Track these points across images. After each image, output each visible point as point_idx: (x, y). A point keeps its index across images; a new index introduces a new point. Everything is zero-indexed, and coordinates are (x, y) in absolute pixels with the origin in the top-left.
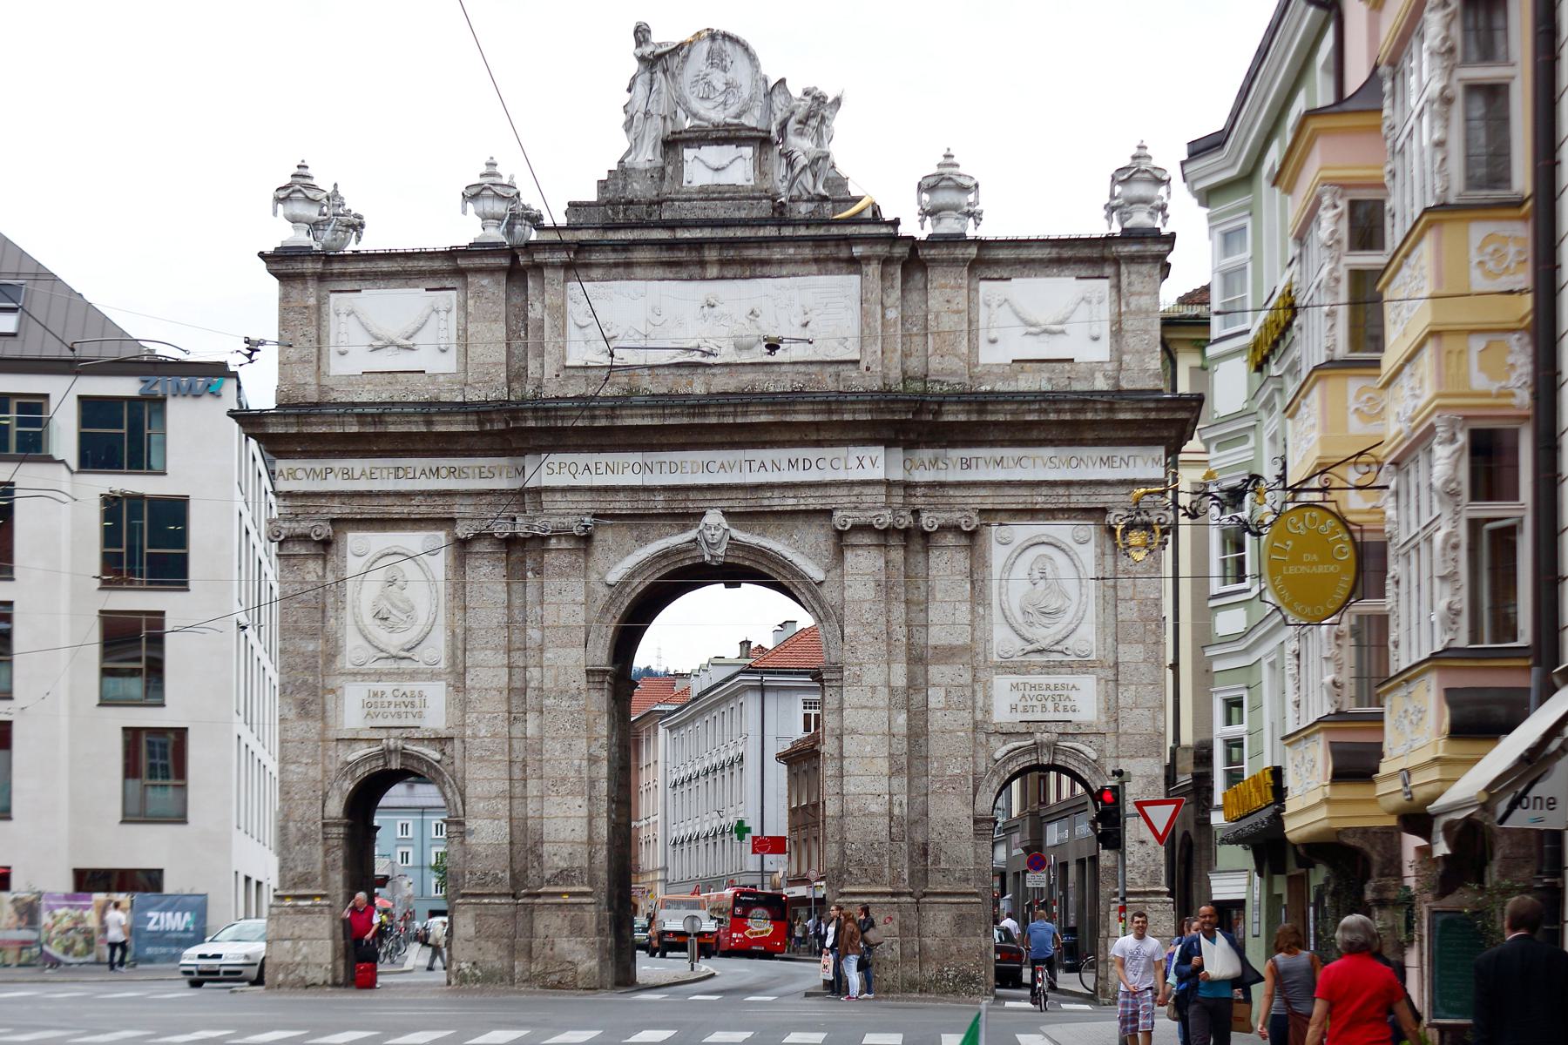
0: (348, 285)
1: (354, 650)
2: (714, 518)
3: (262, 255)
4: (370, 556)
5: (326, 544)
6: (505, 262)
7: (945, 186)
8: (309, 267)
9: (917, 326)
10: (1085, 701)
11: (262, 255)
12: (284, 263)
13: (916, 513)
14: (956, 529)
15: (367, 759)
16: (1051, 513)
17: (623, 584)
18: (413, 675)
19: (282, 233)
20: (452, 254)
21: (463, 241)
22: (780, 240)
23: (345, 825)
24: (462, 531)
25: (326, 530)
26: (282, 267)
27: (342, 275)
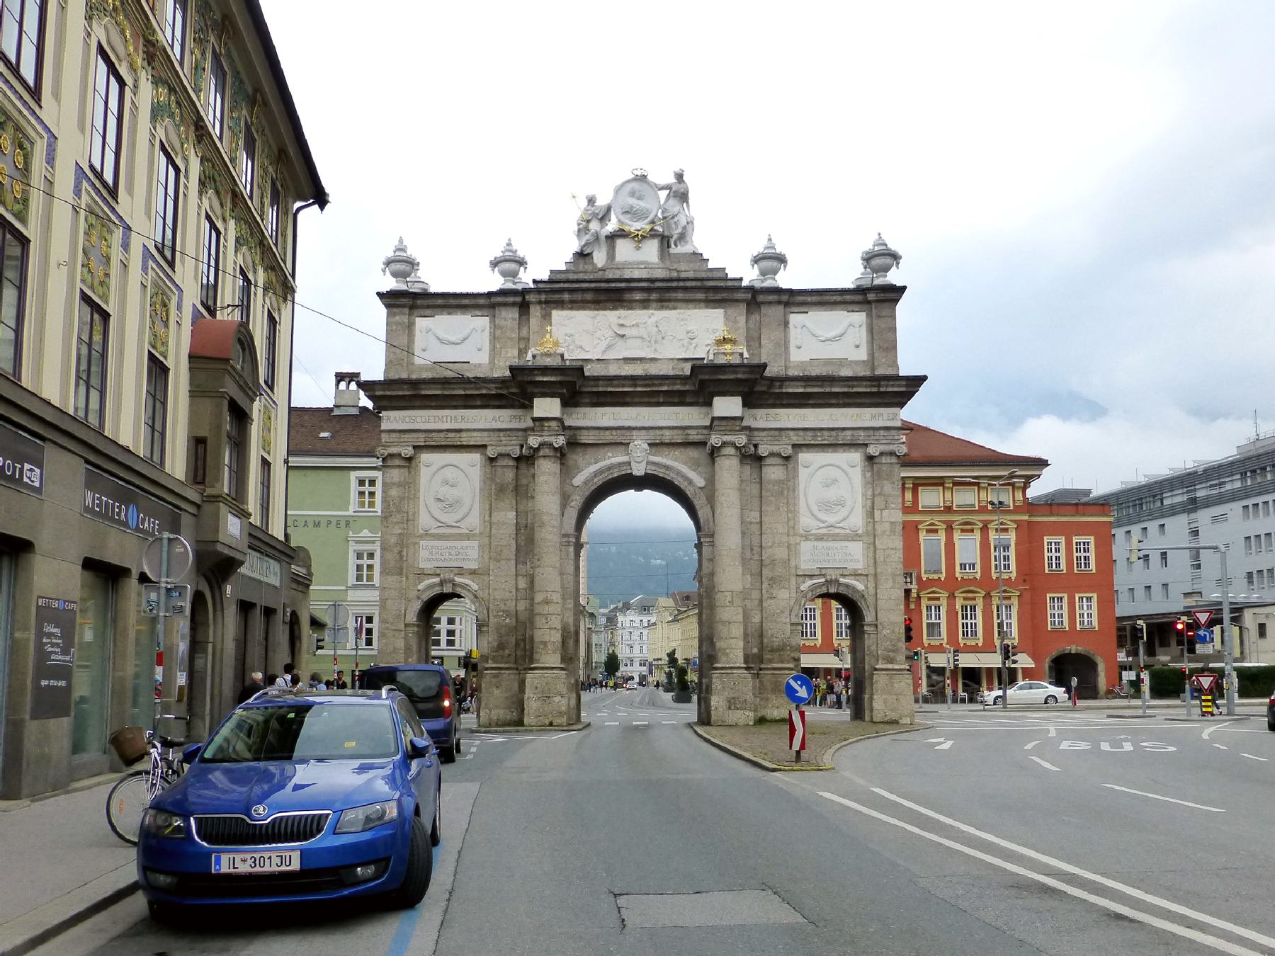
0: (428, 312)
1: (424, 521)
2: (639, 445)
3: (378, 294)
4: (434, 468)
5: (410, 459)
6: (519, 299)
7: (772, 260)
8: (403, 301)
9: (754, 340)
10: (854, 556)
11: (378, 294)
12: (390, 299)
13: (756, 446)
14: (779, 455)
15: (432, 586)
16: (833, 446)
17: (586, 483)
18: (461, 537)
19: (390, 284)
20: (490, 295)
21: (494, 288)
22: (676, 289)
23: (418, 626)
24: (491, 452)
25: (408, 451)
26: (389, 301)
27: (423, 307)
